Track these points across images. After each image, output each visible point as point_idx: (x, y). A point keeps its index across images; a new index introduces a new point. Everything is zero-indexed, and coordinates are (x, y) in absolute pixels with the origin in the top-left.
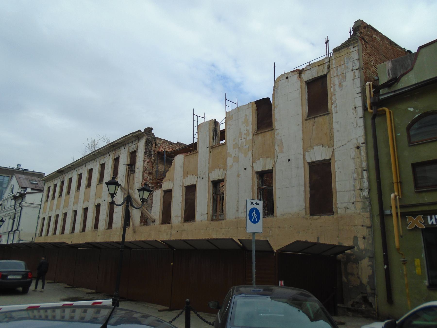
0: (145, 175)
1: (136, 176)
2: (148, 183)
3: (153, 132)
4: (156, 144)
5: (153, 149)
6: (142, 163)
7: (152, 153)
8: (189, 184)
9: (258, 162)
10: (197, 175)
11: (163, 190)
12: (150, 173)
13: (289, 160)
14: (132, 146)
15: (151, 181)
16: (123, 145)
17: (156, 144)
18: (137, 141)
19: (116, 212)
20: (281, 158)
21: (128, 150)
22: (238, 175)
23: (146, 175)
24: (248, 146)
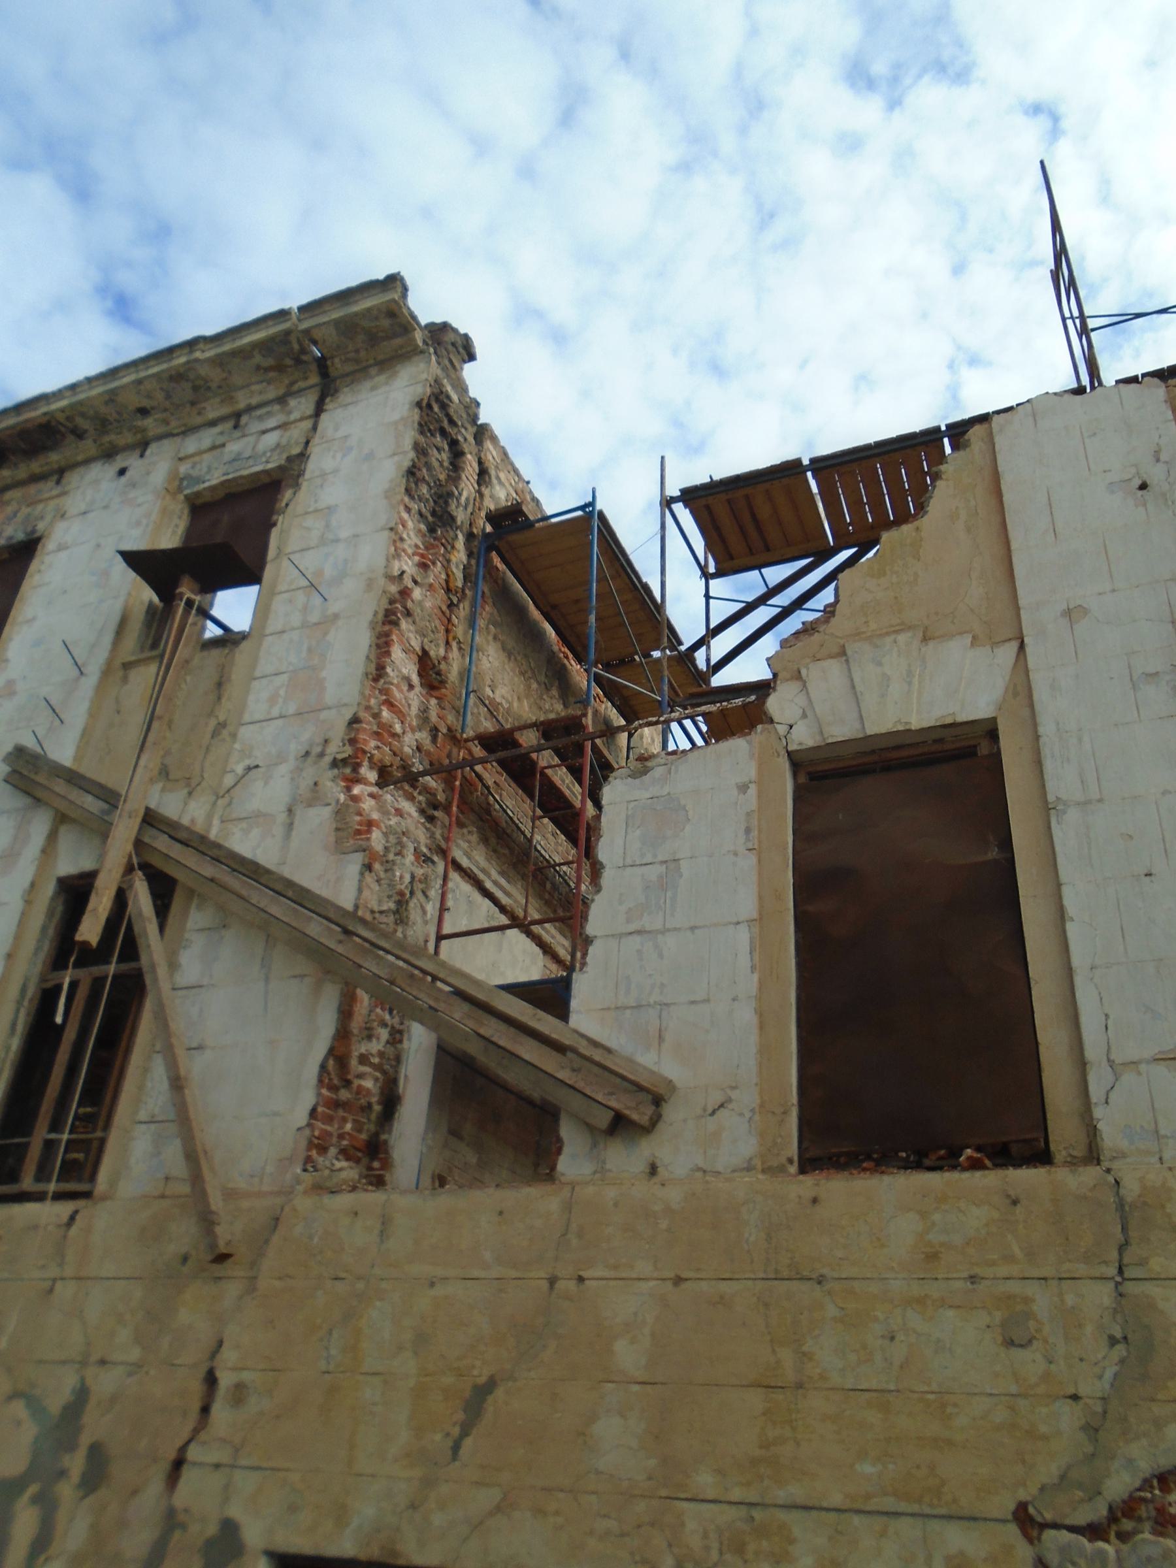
0: (397, 653)
1: (265, 666)
2: (408, 743)
3: (469, 372)
4: (483, 473)
5: (467, 486)
6: (371, 553)
7: (461, 516)
11: (804, 737)
12: (430, 673)
14: (233, 448)
15: (424, 736)
17: (483, 473)
18: (303, 405)
21: (173, 475)
23: (403, 664)
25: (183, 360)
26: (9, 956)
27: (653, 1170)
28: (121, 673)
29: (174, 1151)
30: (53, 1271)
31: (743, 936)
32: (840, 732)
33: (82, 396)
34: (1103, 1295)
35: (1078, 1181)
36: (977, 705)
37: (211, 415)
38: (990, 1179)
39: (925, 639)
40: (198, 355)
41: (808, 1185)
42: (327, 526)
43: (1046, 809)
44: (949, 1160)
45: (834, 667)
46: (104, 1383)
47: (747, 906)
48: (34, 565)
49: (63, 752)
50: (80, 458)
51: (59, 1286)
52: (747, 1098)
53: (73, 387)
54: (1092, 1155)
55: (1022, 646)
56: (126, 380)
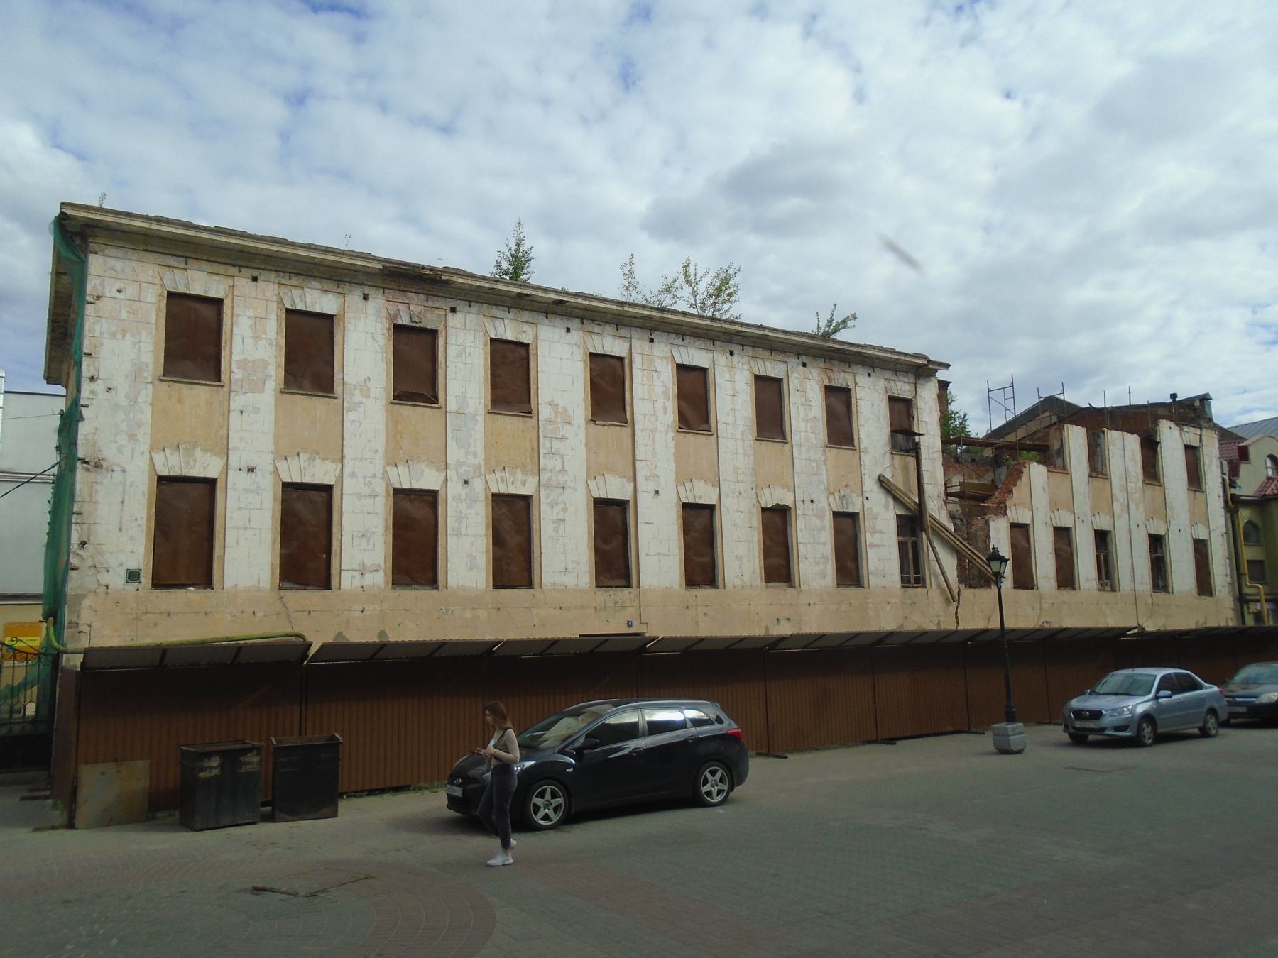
20: (1173, 528)
46: (942, 619)
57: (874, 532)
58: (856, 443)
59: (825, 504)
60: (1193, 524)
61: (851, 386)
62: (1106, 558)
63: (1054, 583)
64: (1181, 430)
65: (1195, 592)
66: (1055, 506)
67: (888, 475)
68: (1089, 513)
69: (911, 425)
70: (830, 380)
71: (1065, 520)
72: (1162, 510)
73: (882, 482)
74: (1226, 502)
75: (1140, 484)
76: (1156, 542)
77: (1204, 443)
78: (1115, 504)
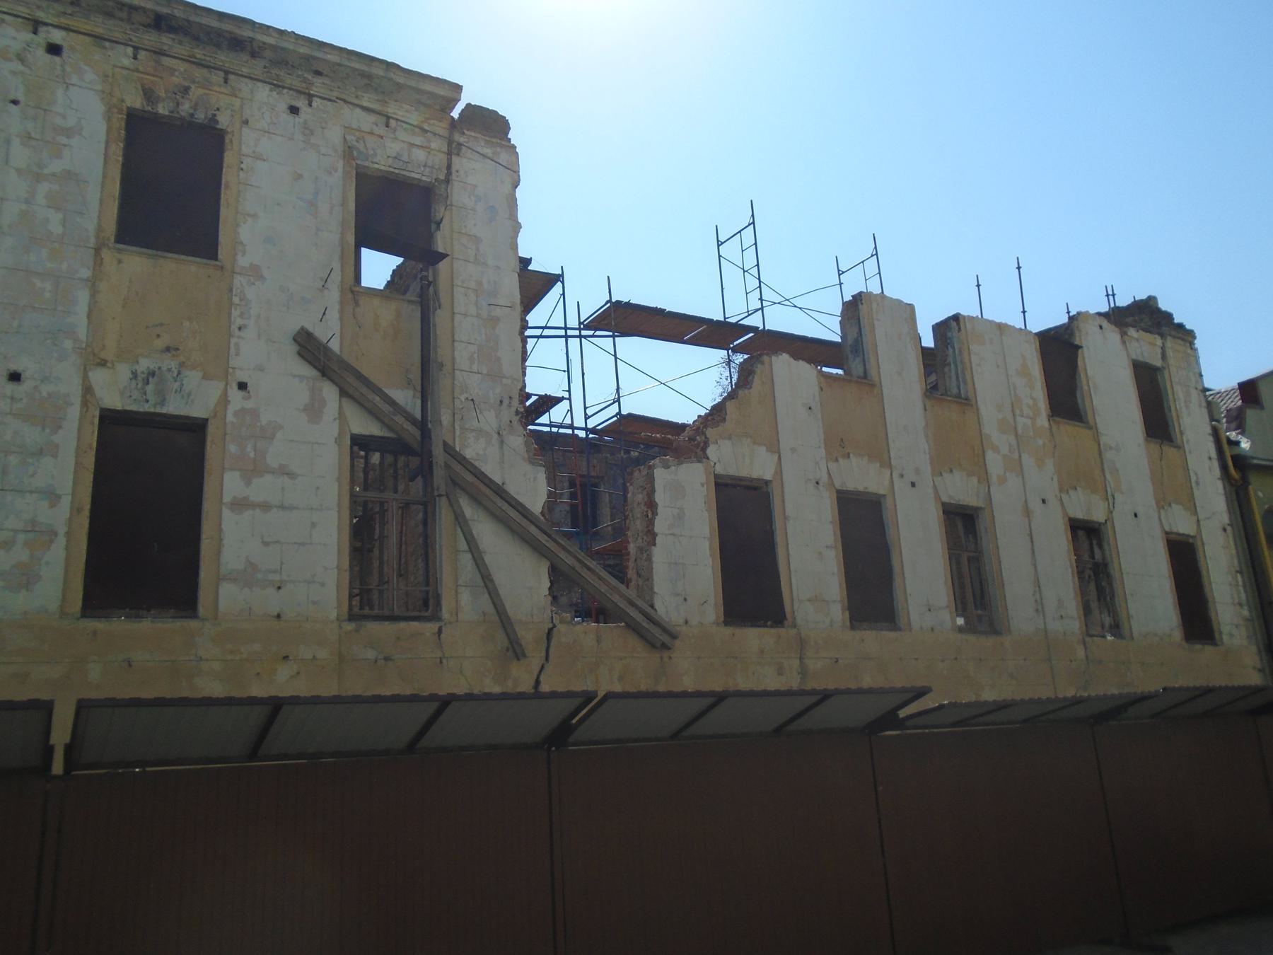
8: (861, 489)
9: (1072, 493)
10: (890, 466)
11: (719, 469)
13: (1136, 515)
16: (278, 86)
19: (240, 505)
22: (1027, 512)
24: (1041, 442)
25: (381, 73)
26: (339, 479)
27: (686, 622)
28: (350, 295)
29: (485, 599)
30: (439, 654)
31: (707, 544)
32: (732, 471)
33: (285, 45)
34: (797, 662)
35: (793, 632)
36: (768, 477)
37: (365, 104)
38: (773, 631)
39: (754, 443)
40: (392, 75)
41: (728, 631)
42: (478, 250)
43: (785, 518)
44: (765, 626)
45: (728, 443)
47: (707, 532)
48: (229, 158)
49: (335, 346)
50: (245, 70)
51: (444, 661)
52: (712, 601)
53: (282, 33)
54: (794, 626)
55: (780, 457)
56: (329, 57)
57: (253, 470)
58: (223, 252)
59: (73, 389)
60: (1162, 503)
61: (223, 120)
62: (977, 560)
63: (838, 613)
64: (1123, 334)
65: (1178, 635)
66: (838, 446)
67: (321, 333)
68: (927, 470)
69: (431, 237)
70: (149, 94)
71: (861, 476)
72: (1089, 472)
73: (308, 347)
74: (1224, 467)
75: (1043, 421)
76: (1087, 534)
77: (1171, 362)
78: (990, 455)
